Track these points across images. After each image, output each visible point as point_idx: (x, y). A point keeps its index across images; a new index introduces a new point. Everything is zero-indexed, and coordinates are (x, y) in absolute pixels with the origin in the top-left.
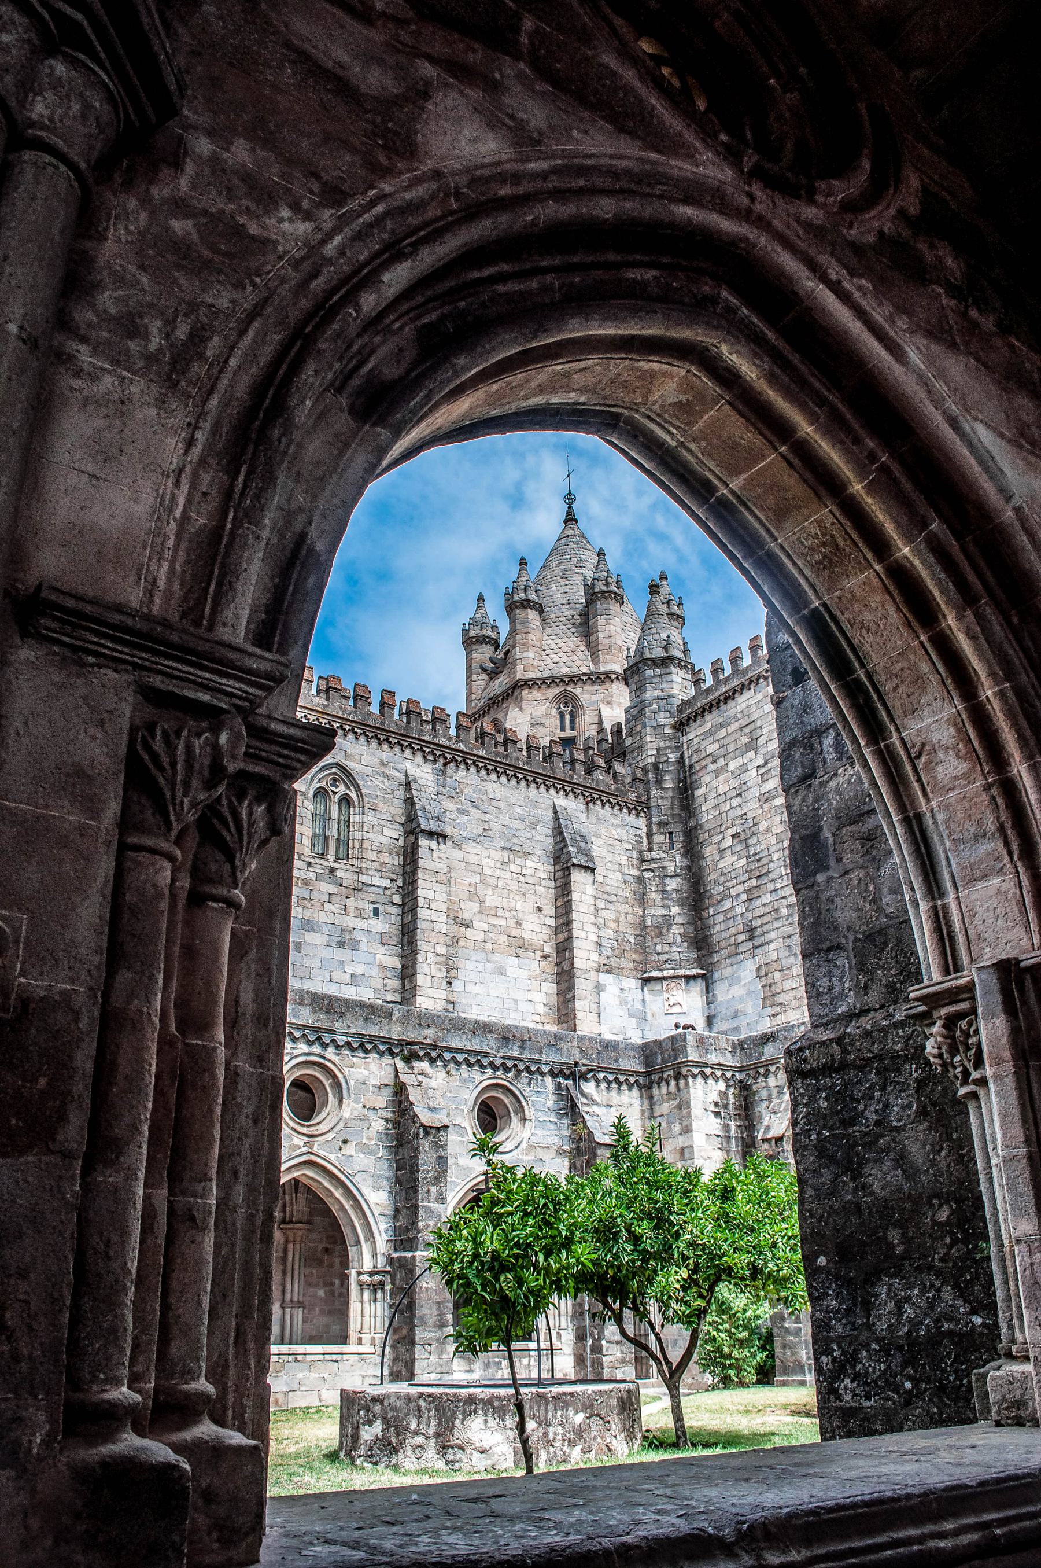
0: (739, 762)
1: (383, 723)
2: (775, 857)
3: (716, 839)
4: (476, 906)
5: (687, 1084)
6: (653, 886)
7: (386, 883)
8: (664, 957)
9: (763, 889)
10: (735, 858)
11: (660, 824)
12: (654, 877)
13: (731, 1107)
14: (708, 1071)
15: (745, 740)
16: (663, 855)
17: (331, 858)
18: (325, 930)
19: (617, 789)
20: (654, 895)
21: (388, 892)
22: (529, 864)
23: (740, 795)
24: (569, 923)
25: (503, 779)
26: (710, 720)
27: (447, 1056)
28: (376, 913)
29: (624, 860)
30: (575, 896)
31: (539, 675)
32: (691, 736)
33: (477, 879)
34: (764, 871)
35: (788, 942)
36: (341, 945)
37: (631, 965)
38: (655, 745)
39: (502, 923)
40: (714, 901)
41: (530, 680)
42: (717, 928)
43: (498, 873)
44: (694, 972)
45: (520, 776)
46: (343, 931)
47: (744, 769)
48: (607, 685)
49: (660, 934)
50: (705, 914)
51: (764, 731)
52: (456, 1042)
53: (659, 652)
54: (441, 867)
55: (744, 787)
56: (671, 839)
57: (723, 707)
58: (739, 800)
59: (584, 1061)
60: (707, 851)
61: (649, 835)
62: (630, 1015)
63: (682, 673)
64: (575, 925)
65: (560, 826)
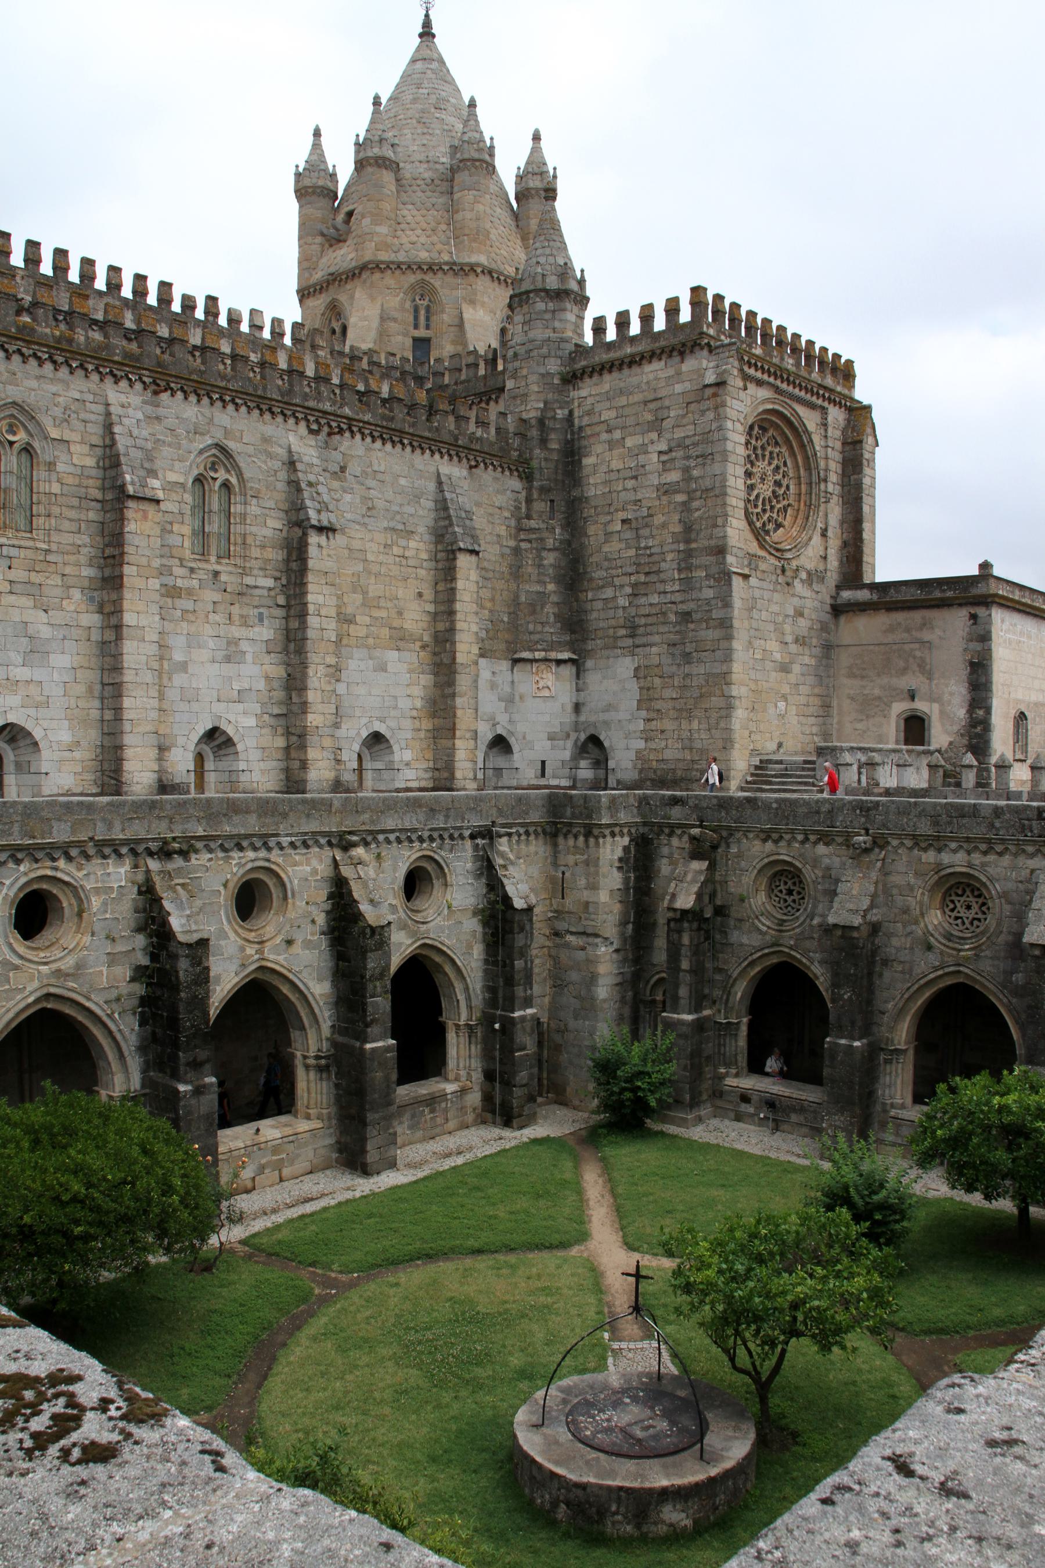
1: (265, 388)
3: (603, 519)
4: (358, 598)
5: (597, 844)
6: (529, 559)
7: (270, 583)
8: (536, 637)
10: (623, 546)
11: (543, 490)
12: (532, 549)
13: (632, 860)
14: (617, 830)
15: (649, 417)
16: (543, 526)
17: (213, 559)
18: (211, 644)
19: (501, 449)
20: (530, 570)
21: (272, 593)
22: (412, 544)
23: (635, 477)
24: (451, 613)
25: (389, 446)
26: (608, 382)
27: (381, 837)
28: (261, 618)
29: (502, 530)
30: (460, 584)
31: (393, 257)
32: (583, 393)
33: (360, 567)
34: (655, 569)
35: (672, 650)
36: (228, 659)
37: (503, 646)
38: (542, 397)
39: (383, 614)
40: (594, 585)
41: (382, 262)
42: (595, 615)
43: (381, 558)
44: (565, 655)
45: (406, 441)
46: (229, 643)
47: (643, 449)
48: (472, 277)
49: (533, 612)
50: (582, 596)
52: (390, 823)
53: (552, 283)
54: (329, 565)
55: (642, 471)
56: (552, 508)
57: (626, 371)
58: (633, 481)
59: (500, 821)
60: (591, 530)
61: (529, 501)
62: (500, 700)
63: (576, 309)
64: (459, 616)
65: (445, 500)
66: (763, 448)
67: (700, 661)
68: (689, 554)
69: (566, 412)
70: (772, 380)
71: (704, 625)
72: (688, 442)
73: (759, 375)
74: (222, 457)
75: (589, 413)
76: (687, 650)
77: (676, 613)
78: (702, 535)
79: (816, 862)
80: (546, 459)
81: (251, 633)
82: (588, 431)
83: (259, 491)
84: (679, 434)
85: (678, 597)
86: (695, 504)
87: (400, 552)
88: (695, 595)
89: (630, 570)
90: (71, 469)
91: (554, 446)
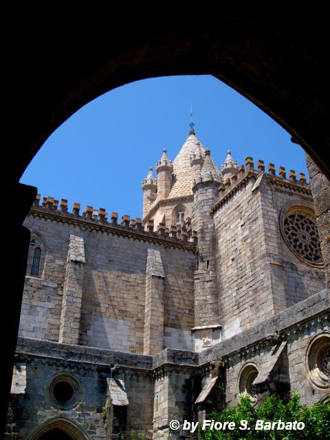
15: (237, 213)
43: (116, 281)
47: (236, 227)
50: (221, 298)
51: (244, 208)
66: (301, 224)
68: (254, 262)
70: (297, 192)
72: (250, 216)
73: (288, 190)
81: (42, 304)
82: (219, 229)
83: (53, 250)
84: (247, 214)
86: (255, 240)
87: (126, 279)
89: (235, 279)
91: (208, 239)
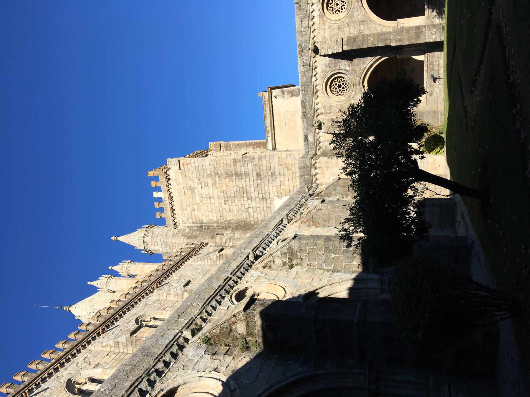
0: (197, 197)
2: (237, 183)
3: (225, 214)
9: (248, 191)
15: (190, 192)
32: (181, 222)
42: (259, 217)
47: (201, 195)
50: (252, 223)
51: (189, 183)
55: (208, 195)
56: (219, 234)
58: (212, 199)
60: (228, 219)
67: (274, 168)
68: (236, 174)
69: (187, 229)
71: (261, 167)
72: (198, 176)
74: (143, 318)
75: (188, 219)
76: (270, 174)
77: (257, 180)
78: (229, 169)
79: (324, 71)
80: (202, 236)
82: (194, 219)
84: (196, 180)
85: (251, 179)
86: (219, 172)
88: (250, 171)
89: (243, 201)
90: (112, 363)
